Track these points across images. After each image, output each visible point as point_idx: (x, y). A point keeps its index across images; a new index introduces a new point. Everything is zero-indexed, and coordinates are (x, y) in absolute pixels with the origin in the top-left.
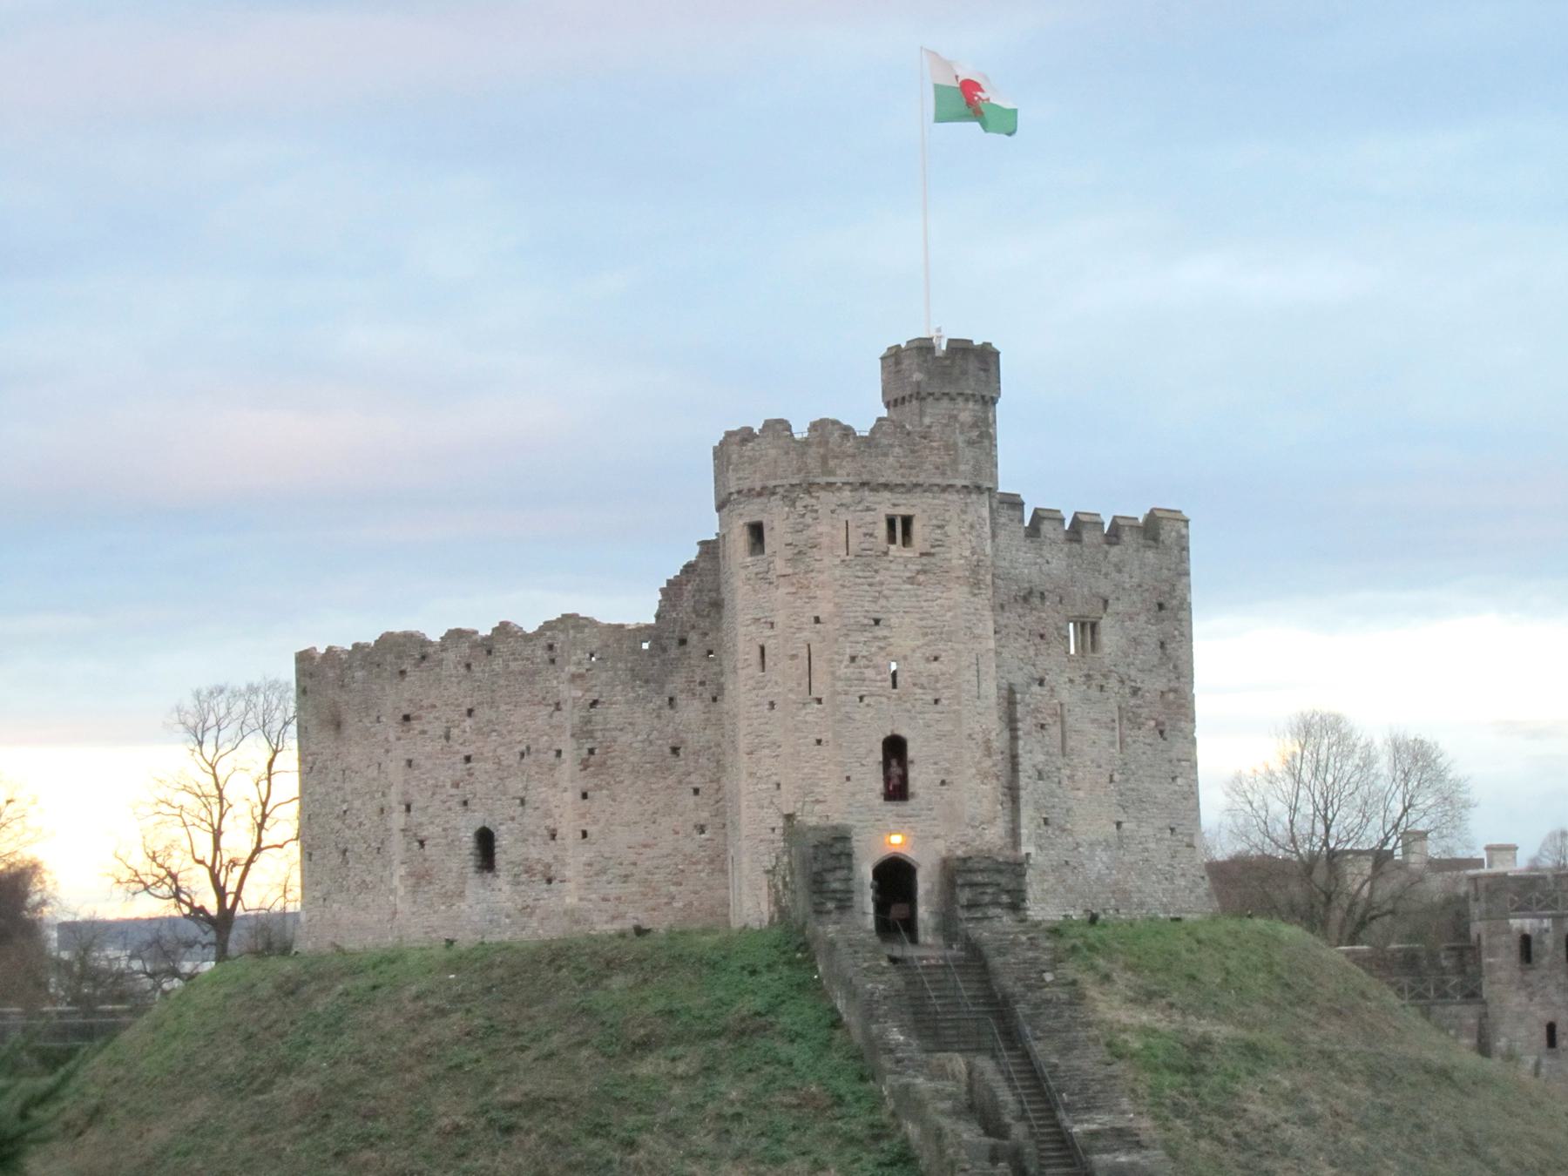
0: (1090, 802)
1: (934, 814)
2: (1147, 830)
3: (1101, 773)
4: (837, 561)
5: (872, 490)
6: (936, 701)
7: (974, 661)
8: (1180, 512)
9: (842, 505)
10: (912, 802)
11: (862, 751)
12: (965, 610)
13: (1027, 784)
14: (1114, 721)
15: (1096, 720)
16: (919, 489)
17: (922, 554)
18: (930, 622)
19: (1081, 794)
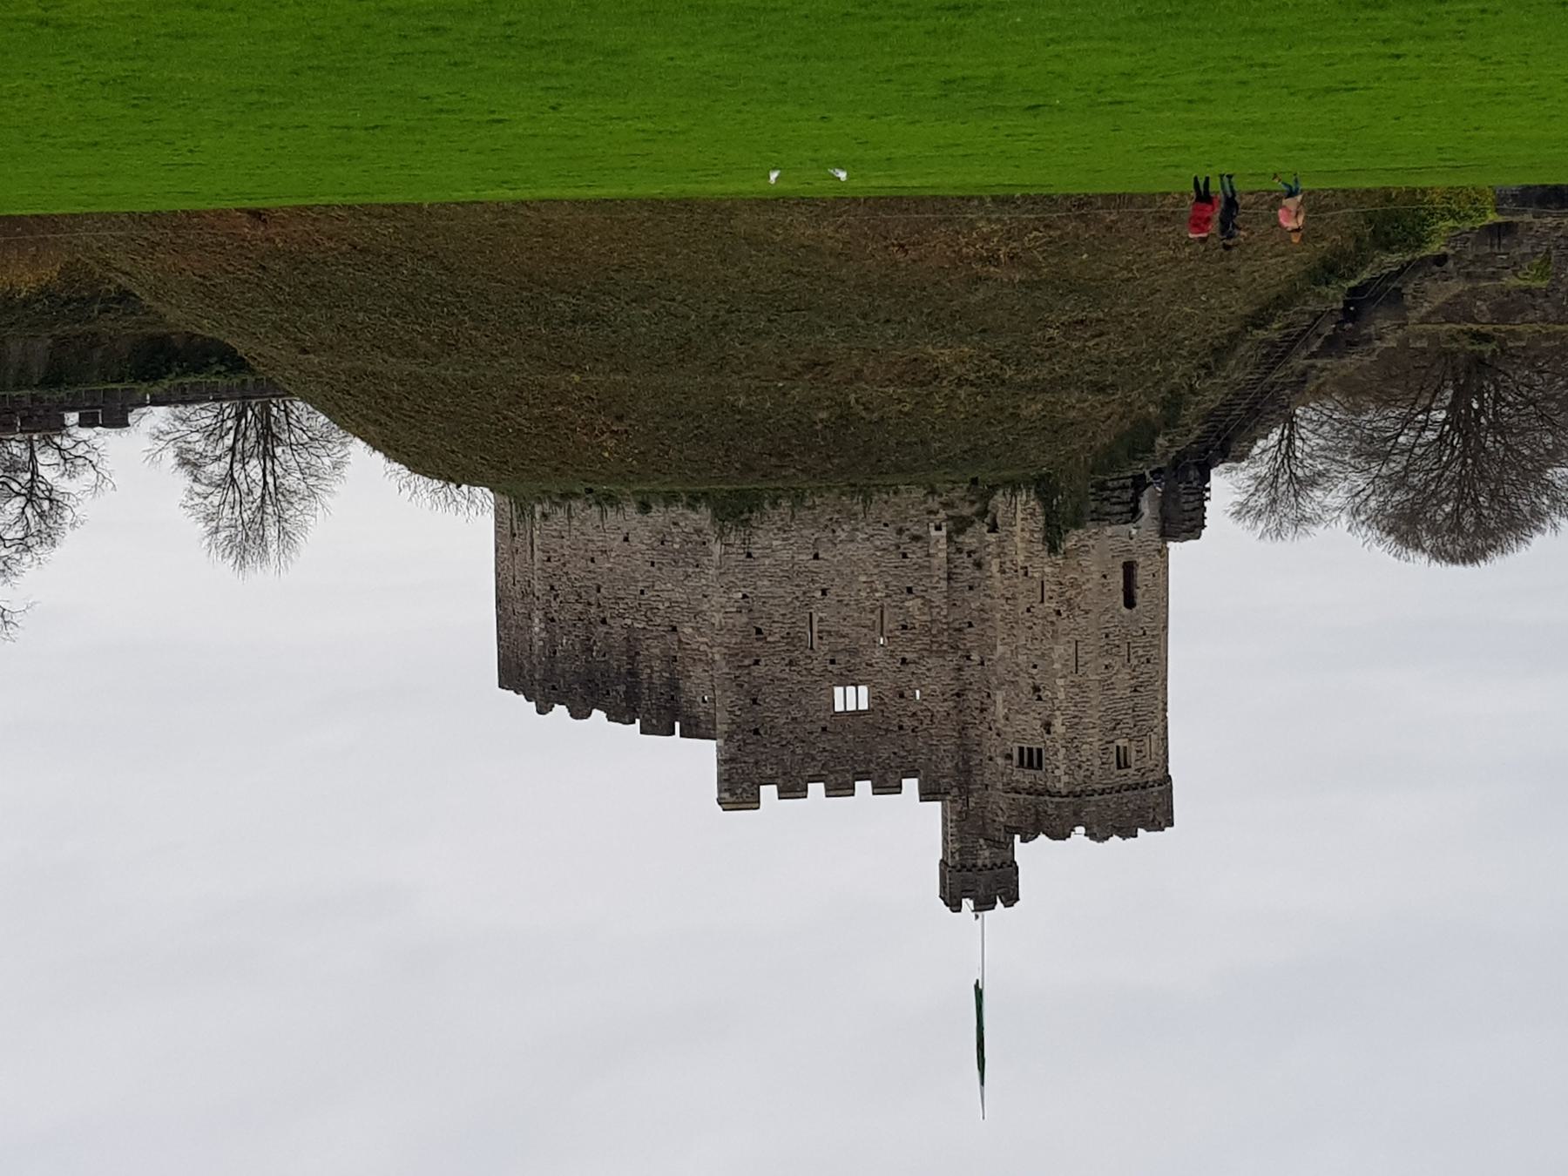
0: (853, 572)
1: (1111, 553)
2: (785, 555)
3: (838, 596)
4: (1155, 730)
5: (1138, 784)
6: (1107, 636)
7: (1080, 668)
8: (724, 810)
9: (1152, 771)
10: (1123, 560)
11: (1147, 596)
12: (1088, 705)
13: (938, 582)
14: (821, 638)
15: (844, 637)
16: (1117, 788)
17: (1112, 742)
18: (1109, 692)
19: (863, 579)
